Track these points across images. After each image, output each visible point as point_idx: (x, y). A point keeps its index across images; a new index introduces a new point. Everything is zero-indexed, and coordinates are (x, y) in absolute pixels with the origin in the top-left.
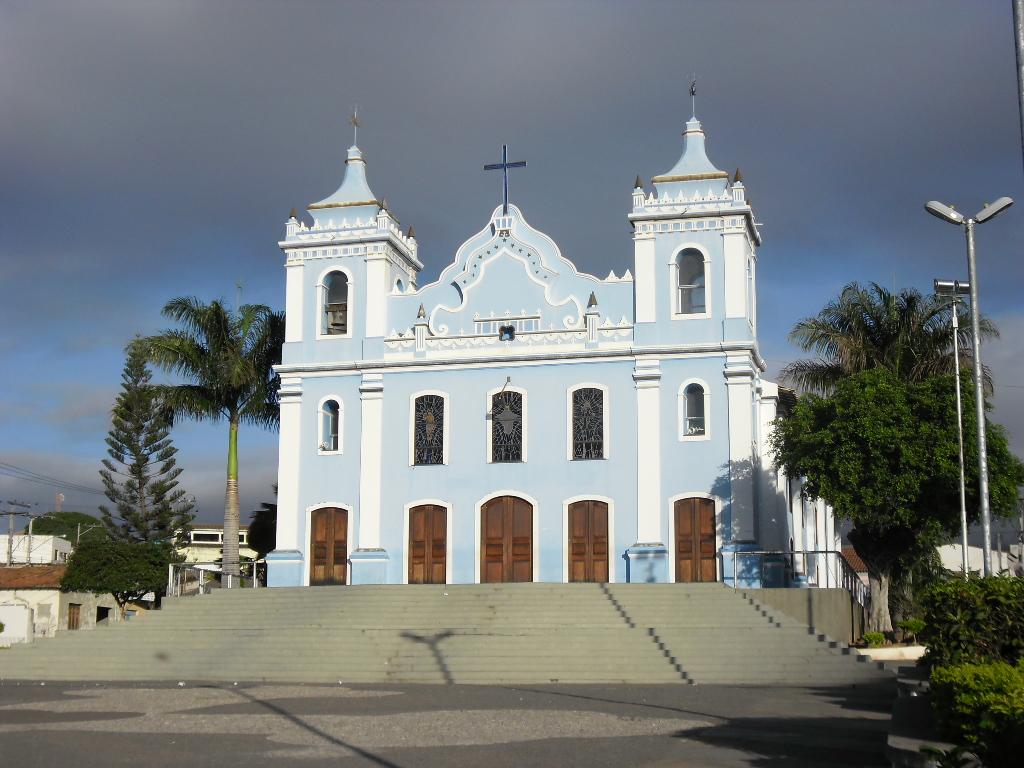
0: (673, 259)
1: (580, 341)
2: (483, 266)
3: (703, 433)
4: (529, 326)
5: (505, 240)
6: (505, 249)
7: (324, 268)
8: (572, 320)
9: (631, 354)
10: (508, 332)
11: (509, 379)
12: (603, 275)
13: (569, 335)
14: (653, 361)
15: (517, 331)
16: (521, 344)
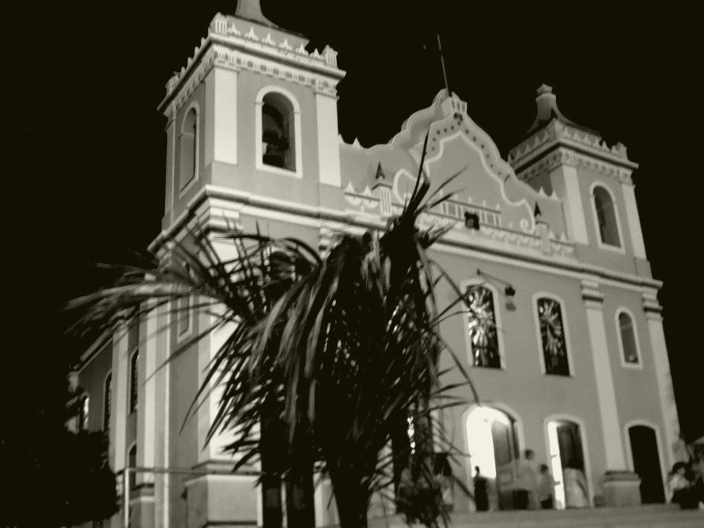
0: (591, 191)
1: (538, 248)
2: (443, 141)
3: (636, 361)
4: (490, 219)
5: (459, 124)
6: (459, 133)
7: (263, 86)
8: (527, 225)
9: (582, 271)
10: (473, 221)
11: (479, 273)
12: (537, 189)
13: (526, 240)
14: (595, 281)
15: (481, 221)
16: (484, 236)
